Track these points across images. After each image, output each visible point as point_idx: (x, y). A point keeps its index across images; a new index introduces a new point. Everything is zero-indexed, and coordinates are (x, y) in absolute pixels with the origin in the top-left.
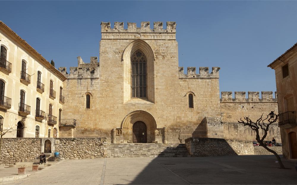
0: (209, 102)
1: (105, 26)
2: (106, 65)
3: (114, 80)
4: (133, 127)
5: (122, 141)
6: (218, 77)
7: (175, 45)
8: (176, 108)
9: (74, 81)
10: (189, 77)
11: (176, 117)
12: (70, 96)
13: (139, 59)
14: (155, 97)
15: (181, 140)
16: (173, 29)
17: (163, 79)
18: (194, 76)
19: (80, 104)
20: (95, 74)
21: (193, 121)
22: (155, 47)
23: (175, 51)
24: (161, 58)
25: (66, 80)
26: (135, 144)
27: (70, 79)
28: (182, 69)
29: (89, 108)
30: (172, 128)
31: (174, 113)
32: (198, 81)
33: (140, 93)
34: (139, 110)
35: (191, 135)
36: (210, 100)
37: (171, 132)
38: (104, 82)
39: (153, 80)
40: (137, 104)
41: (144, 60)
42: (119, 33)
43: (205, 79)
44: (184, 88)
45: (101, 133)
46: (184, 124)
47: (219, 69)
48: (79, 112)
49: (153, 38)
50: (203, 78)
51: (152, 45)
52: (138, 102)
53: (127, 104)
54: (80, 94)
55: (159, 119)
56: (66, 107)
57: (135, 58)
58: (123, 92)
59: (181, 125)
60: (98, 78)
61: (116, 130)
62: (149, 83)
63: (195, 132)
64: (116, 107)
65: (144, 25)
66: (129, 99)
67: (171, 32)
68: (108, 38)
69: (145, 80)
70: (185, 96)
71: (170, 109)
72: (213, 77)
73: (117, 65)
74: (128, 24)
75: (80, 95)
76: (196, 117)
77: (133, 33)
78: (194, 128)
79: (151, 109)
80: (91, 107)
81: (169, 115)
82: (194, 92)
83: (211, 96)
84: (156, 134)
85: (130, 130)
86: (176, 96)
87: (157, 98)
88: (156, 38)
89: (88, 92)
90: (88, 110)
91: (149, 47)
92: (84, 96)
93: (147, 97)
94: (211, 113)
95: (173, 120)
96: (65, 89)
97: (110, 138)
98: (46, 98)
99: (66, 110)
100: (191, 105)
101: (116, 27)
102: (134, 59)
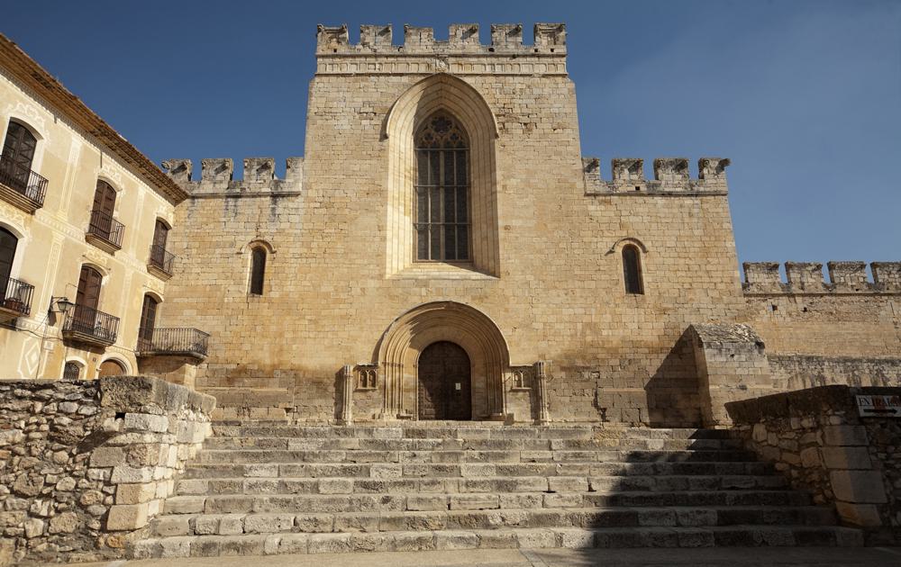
0: (700, 274)
1: (331, 38)
3: (354, 199)
4: (422, 361)
5: (377, 411)
6: (724, 189)
7: (565, 91)
8: (578, 295)
9: (213, 202)
10: (621, 190)
11: (579, 326)
12: (194, 251)
13: (442, 137)
14: (501, 257)
15: (605, 409)
16: (555, 44)
17: (527, 197)
18: (638, 188)
19: (227, 278)
21: (644, 338)
22: (498, 96)
23: (568, 110)
25: (187, 201)
27: (197, 198)
28: (593, 165)
29: (261, 293)
34: (441, 299)
35: (642, 390)
36: (703, 267)
39: (493, 203)
40: (435, 279)
42: (376, 56)
43: (678, 195)
44: (604, 227)
45: (298, 382)
46: (613, 352)
47: (723, 164)
48: (220, 306)
49: (488, 70)
50: (670, 194)
52: (438, 273)
53: (396, 281)
54: (232, 245)
55: (516, 333)
57: (429, 136)
58: (384, 239)
59: (599, 356)
60: (297, 195)
61: (354, 370)
62: (477, 212)
63: (654, 380)
64: (359, 291)
65: (460, 33)
66: (407, 265)
67: (550, 52)
68: (337, 71)
69: (465, 203)
70: (611, 252)
71: (559, 296)
72: (708, 189)
73: (364, 153)
74: (406, 32)
75: (228, 251)
76: (655, 325)
77: (423, 56)
78: (653, 365)
79: (487, 297)
80: (265, 290)
81: (552, 319)
82: (641, 239)
83: (705, 251)
84: (508, 389)
85: (409, 373)
86: (576, 251)
87: (508, 258)
88: (498, 70)
89: (259, 238)
90: (256, 299)
92: (243, 251)
94: (710, 313)
95: (572, 336)
96: (181, 229)
97: (334, 401)
99: (175, 300)
100: (634, 284)
101: (366, 41)
102: (426, 139)
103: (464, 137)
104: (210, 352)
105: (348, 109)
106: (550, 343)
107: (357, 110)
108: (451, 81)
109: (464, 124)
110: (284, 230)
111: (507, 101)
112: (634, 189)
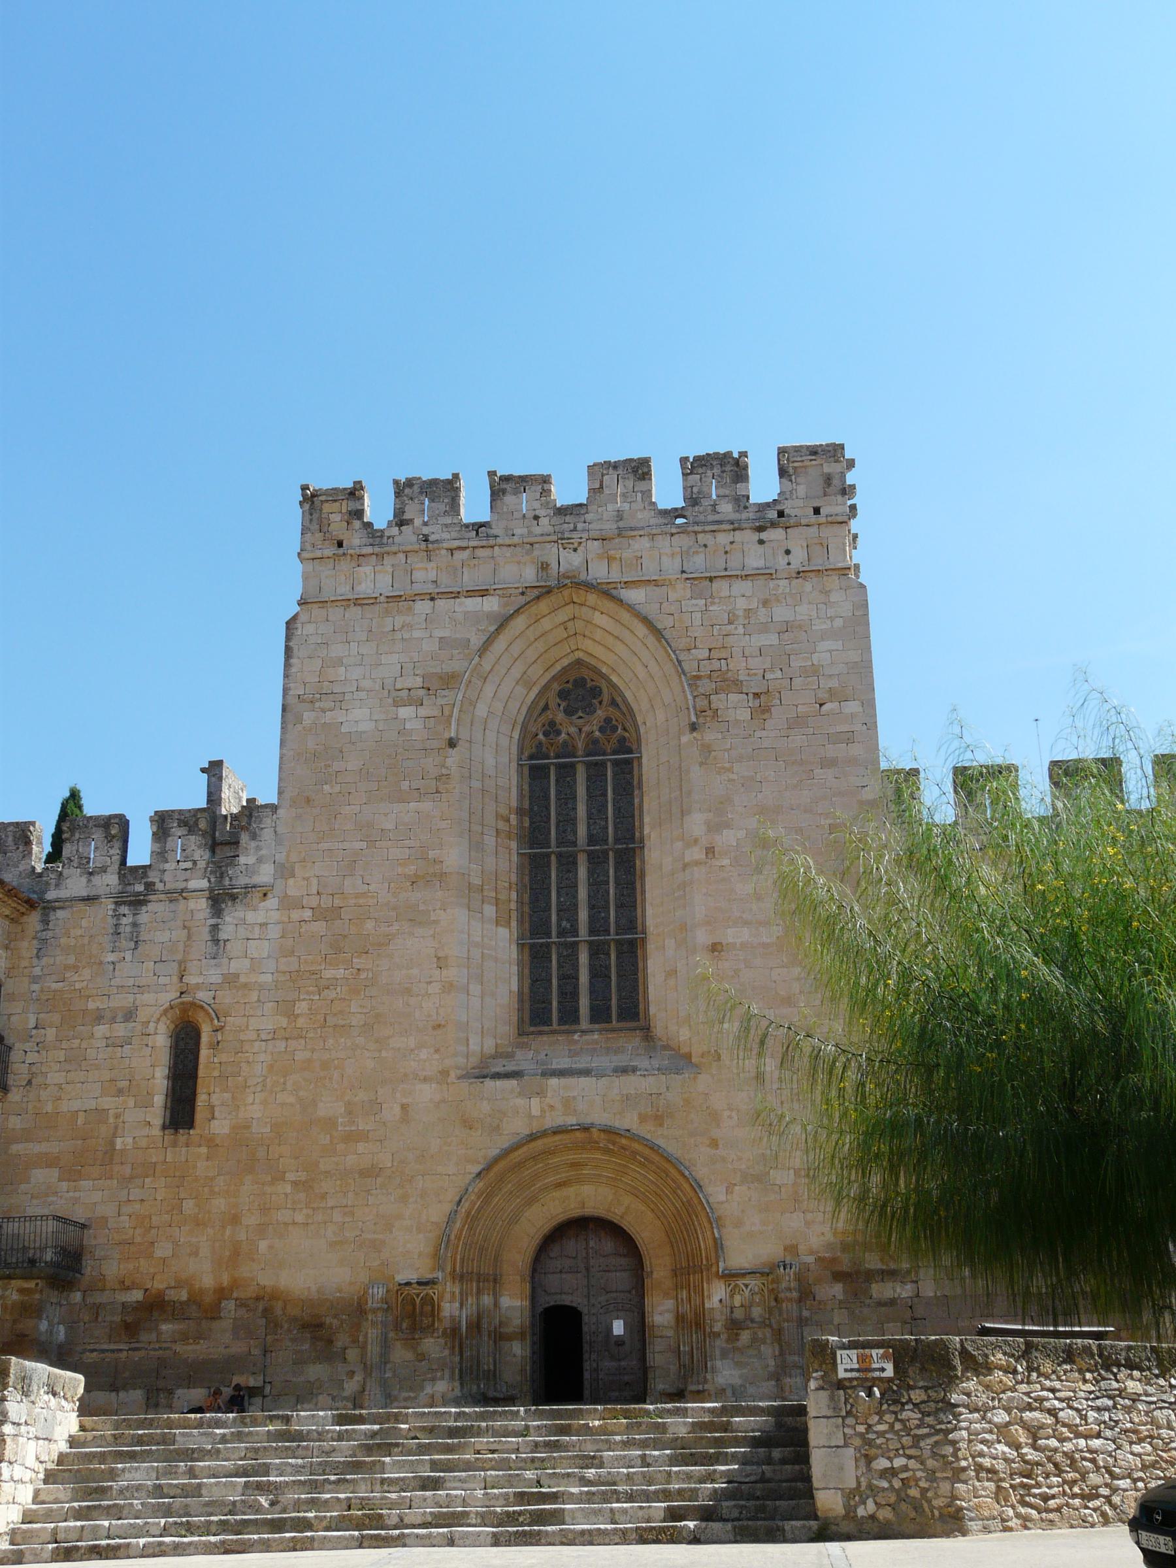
12: (51, 1033)
13: (580, 730)
19: (120, 1092)
20: (242, 860)
22: (698, 632)
29: (190, 1124)
30: (845, 1265)
33: (592, 991)
34: (572, 1120)
38: (307, 914)
54: (130, 1015)
57: (552, 729)
64: (397, 1109)
68: (344, 590)
69: (634, 883)
73: (405, 785)
75: (120, 1030)
80: (200, 1115)
89: (187, 998)
91: (651, 640)
99: (15, 1148)
101: (407, 516)
102: (546, 734)
103: (628, 725)
105: (366, 684)
106: (809, 1216)
108: (592, 598)
109: (628, 694)
110: (237, 976)
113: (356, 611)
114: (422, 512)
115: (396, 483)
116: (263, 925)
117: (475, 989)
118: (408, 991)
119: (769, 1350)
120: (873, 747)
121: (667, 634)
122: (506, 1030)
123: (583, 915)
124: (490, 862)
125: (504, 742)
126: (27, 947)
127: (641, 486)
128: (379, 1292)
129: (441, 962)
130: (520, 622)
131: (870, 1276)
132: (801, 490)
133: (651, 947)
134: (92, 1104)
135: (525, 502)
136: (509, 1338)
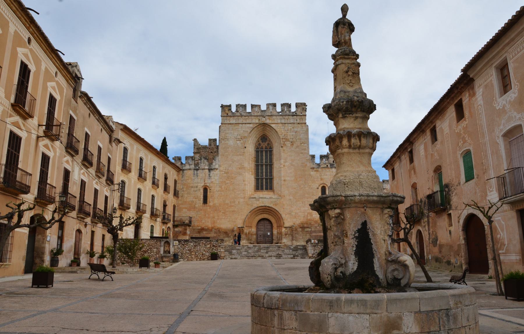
2: (226, 153)
8: (306, 203)
10: (322, 166)
11: (306, 214)
12: (185, 189)
18: (327, 166)
19: (196, 198)
20: (213, 164)
24: (290, 145)
25: (181, 172)
26: (254, 246)
30: (302, 226)
31: (304, 209)
32: (332, 170)
33: (266, 185)
34: (263, 205)
37: (301, 231)
38: (224, 173)
41: (270, 147)
48: (195, 208)
49: (279, 121)
51: (279, 130)
54: (197, 187)
56: (180, 202)
57: (260, 144)
59: (312, 223)
64: (237, 202)
68: (228, 122)
69: (272, 170)
70: (318, 188)
75: (195, 189)
79: (277, 204)
80: (208, 202)
88: (283, 121)
90: (205, 205)
93: (274, 189)
98: (160, 194)
99: (180, 206)
101: (238, 110)
104: (192, 223)
105: (232, 137)
107: (235, 137)
108: (267, 125)
109: (272, 141)
111: (286, 133)
112: (326, 166)
113: (230, 125)
114: (241, 109)
115: (236, 105)
116: (217, 174)
117: (249, 185)
118: (239, 185)
119: (291, 238)
120: (309, 152)
121: (278, 132)
122: (253, 191)
123: (264, 174)
124: (251, 166)
125: (253, 147)
126: (180, 176)
127: (275, 108)
128: (236, 228)
129: (244, 181)
130: (256, 128)
131: (305, 228)
132: (299, 110)
133: (274, 179)
134: (192, 200)
135: (256, 109)
136: (253, 235)
